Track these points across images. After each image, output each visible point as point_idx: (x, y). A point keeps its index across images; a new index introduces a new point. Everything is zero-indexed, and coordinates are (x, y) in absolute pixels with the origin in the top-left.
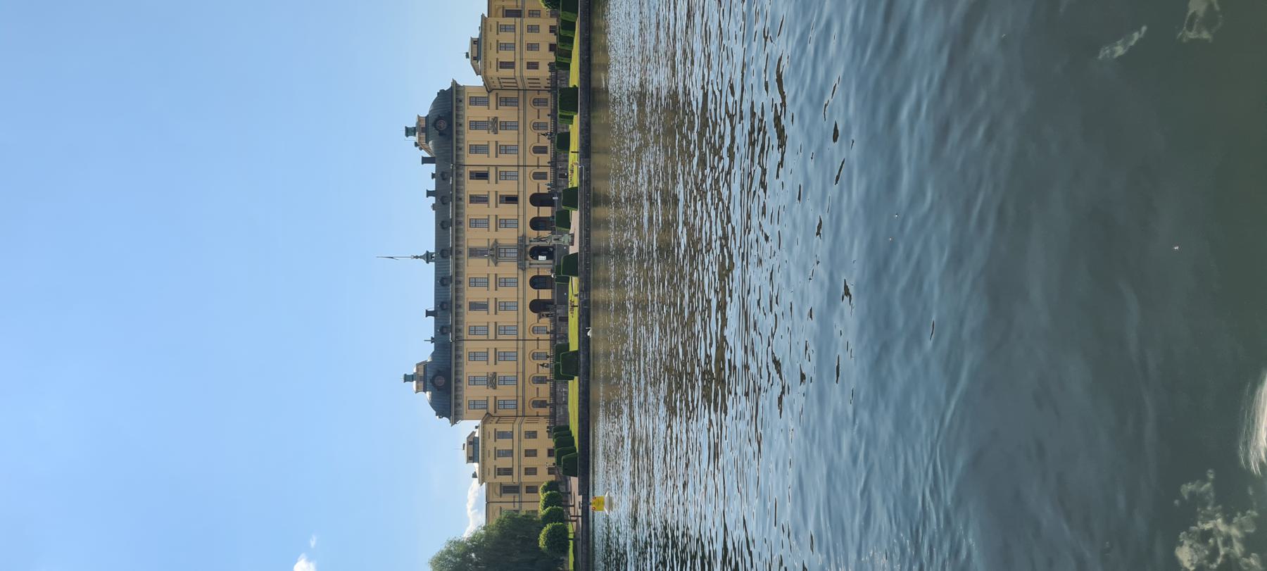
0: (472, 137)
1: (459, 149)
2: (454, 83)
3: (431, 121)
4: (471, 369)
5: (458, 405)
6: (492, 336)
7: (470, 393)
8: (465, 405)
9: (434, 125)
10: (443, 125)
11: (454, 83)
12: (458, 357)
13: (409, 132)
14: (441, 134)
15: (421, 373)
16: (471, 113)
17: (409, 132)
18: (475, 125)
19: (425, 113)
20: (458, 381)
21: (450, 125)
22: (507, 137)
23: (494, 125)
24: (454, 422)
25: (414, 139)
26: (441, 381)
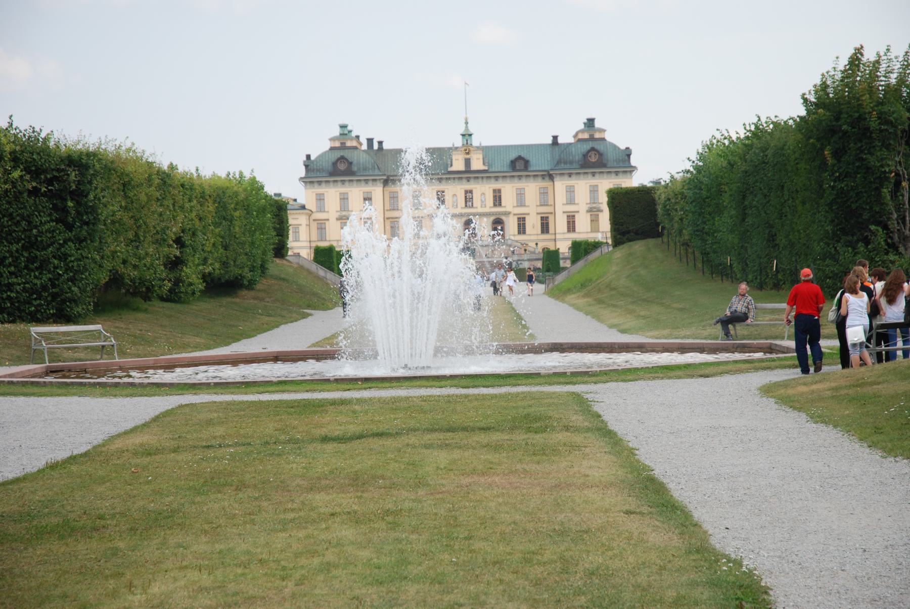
1: (570, 175)
3: (599, 147)
4: (355, 192)
5: (320, 183)
6: (388, 214)
7: (332, 194)
8: (320, 190)
9: (593, 149)
10: (593, 159)
12: (366, 181)
13: (590, 122)
14: (585, 156)
15: (349, 144)
17: (590, 122)
19: (609, 137)
20: (343, 182)
26: (342, 167)
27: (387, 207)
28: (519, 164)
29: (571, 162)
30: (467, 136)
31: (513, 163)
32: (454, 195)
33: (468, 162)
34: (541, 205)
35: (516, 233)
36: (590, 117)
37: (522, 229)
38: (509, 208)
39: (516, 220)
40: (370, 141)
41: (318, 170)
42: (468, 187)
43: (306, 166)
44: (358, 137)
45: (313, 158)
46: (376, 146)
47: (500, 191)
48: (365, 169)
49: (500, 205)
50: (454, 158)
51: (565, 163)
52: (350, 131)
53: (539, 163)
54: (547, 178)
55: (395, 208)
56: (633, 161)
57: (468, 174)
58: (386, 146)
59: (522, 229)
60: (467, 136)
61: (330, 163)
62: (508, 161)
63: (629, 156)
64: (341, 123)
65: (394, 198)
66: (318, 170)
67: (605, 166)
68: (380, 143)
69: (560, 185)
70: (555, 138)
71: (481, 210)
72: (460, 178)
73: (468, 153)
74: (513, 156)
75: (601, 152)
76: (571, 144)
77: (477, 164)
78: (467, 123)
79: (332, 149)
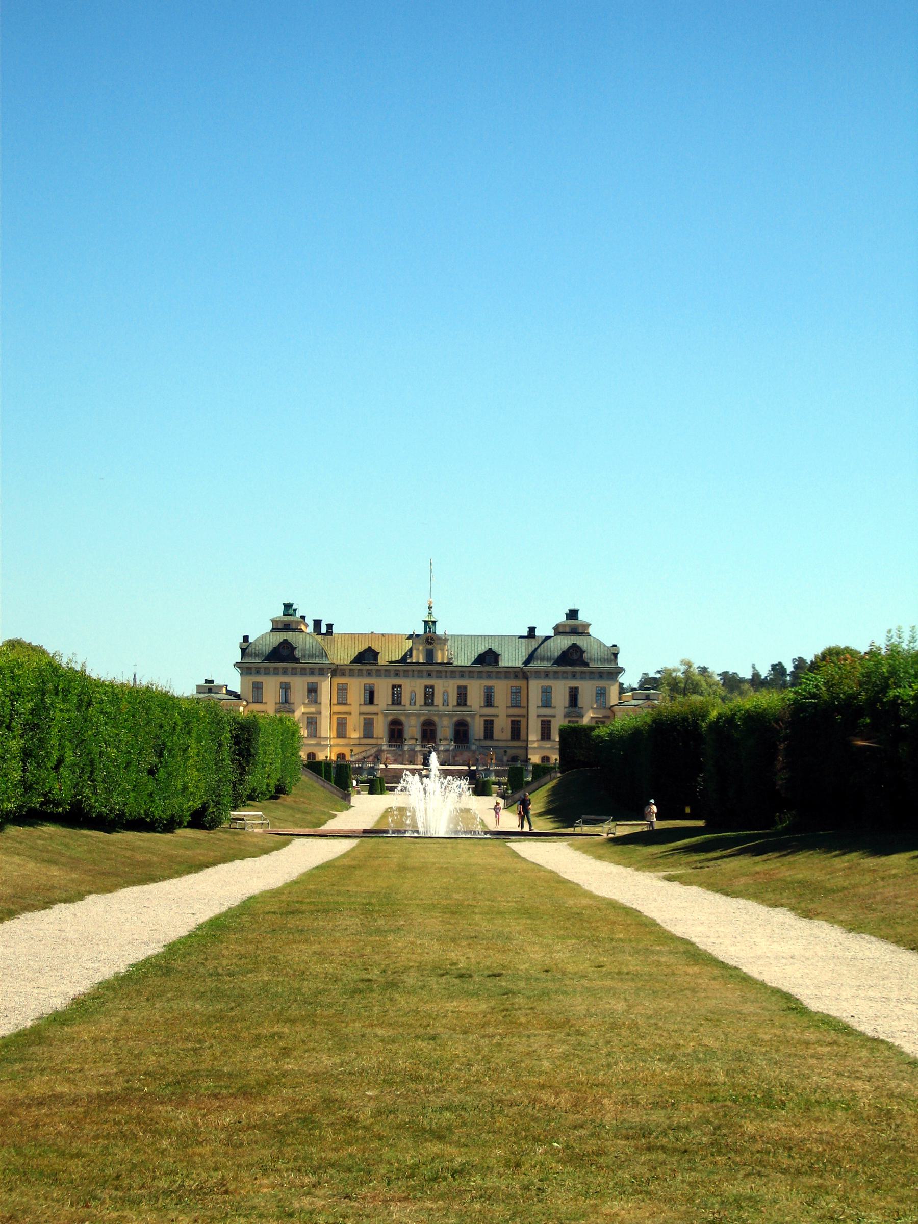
1: (547, 675)
4: (299, 684)
5: (258, 671)
8: (258, 679)
12: (312, 672)
13: (573, 614)
16: (587, 689)
17: (573, 614)
21: (572, 663)
24: (237, 665)
27: (335, 701)
28: (488, 658)
29: (548, 659)
30: (429, 624)
32: (413, 692)
33: (430, 655)
34: (512, 707)
35: (482, 738)
36: (572, 608)
39: (483, 723)
40: (317, 623)
43: (243, 650)
44: (303, 617)
45: (251, 640)
46: (324, 630)
47: (465, 688)
48: (311, 656)
49: (465, 705)
51: (542, 659)
52: (295, 610)
53: (512, 658)
55: (342, 702)
56: (621, 662)
58: (335, 630)
60: (429, 624)
62: (477, 655)
63: (615, 655)
65: (343, 689)
66: (257, 655)
67: (587, 665)
68: (330, 626)
69: (535, 687)
70: (532, 630)
72: (420, 674)
73: (430, 643)
74: (483, 649)
75: (584, 649)
76: (548, 638)
78: (430, 608)
79: (274, 630)
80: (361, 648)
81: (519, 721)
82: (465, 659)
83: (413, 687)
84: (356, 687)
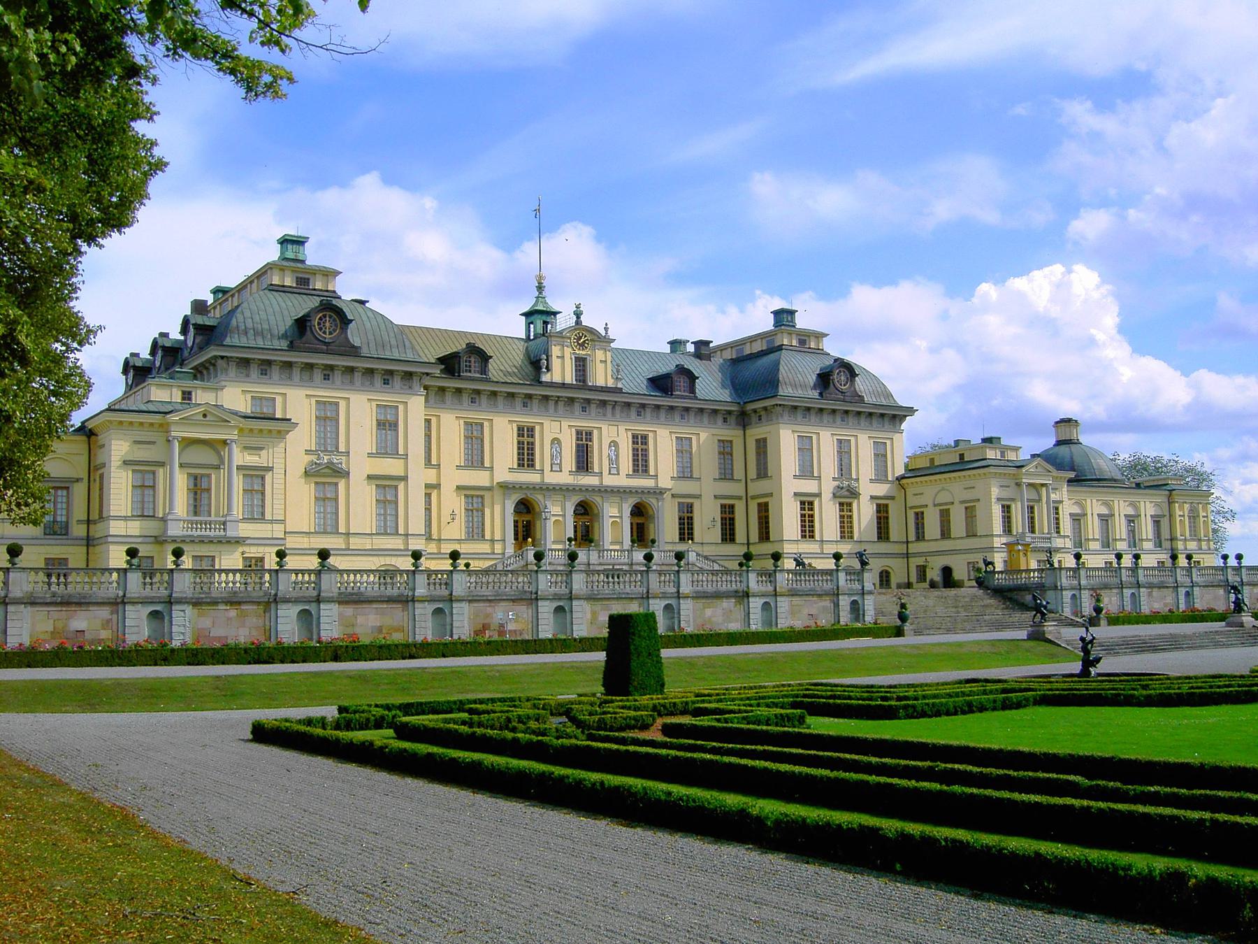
0: (826, 440)
2: (911, 411)
4: (360, 409)
7: (298, 401)
11: (911, 411)
16: (863, 443)
17: (783, 317)
18: (844, 451)
22: (828, 518)
23: (846, 497)
25: (768, 324)
28: (669, 386)
29: (803, 386)
30: (539, 315)
31: (661, 384)
33: (581, 365)
37: (686, 530)
38: (665, 482)
41: (258, 333)
42: (585, 424)
47: (645, 438)
50: (555, 351)
51: (795, 386)
54: (732, 419)
57: (583, 397)
59: (686, 530)
61: (289, 322)
64: (292, 231)
71: (609, 481)
73: (582, 346)
77: (601, 376)
78: (540, 288)
80: (459, 346)
81: (732, 507)
82: (635, 383)
83: (556, 432)
84: (451, 425)
